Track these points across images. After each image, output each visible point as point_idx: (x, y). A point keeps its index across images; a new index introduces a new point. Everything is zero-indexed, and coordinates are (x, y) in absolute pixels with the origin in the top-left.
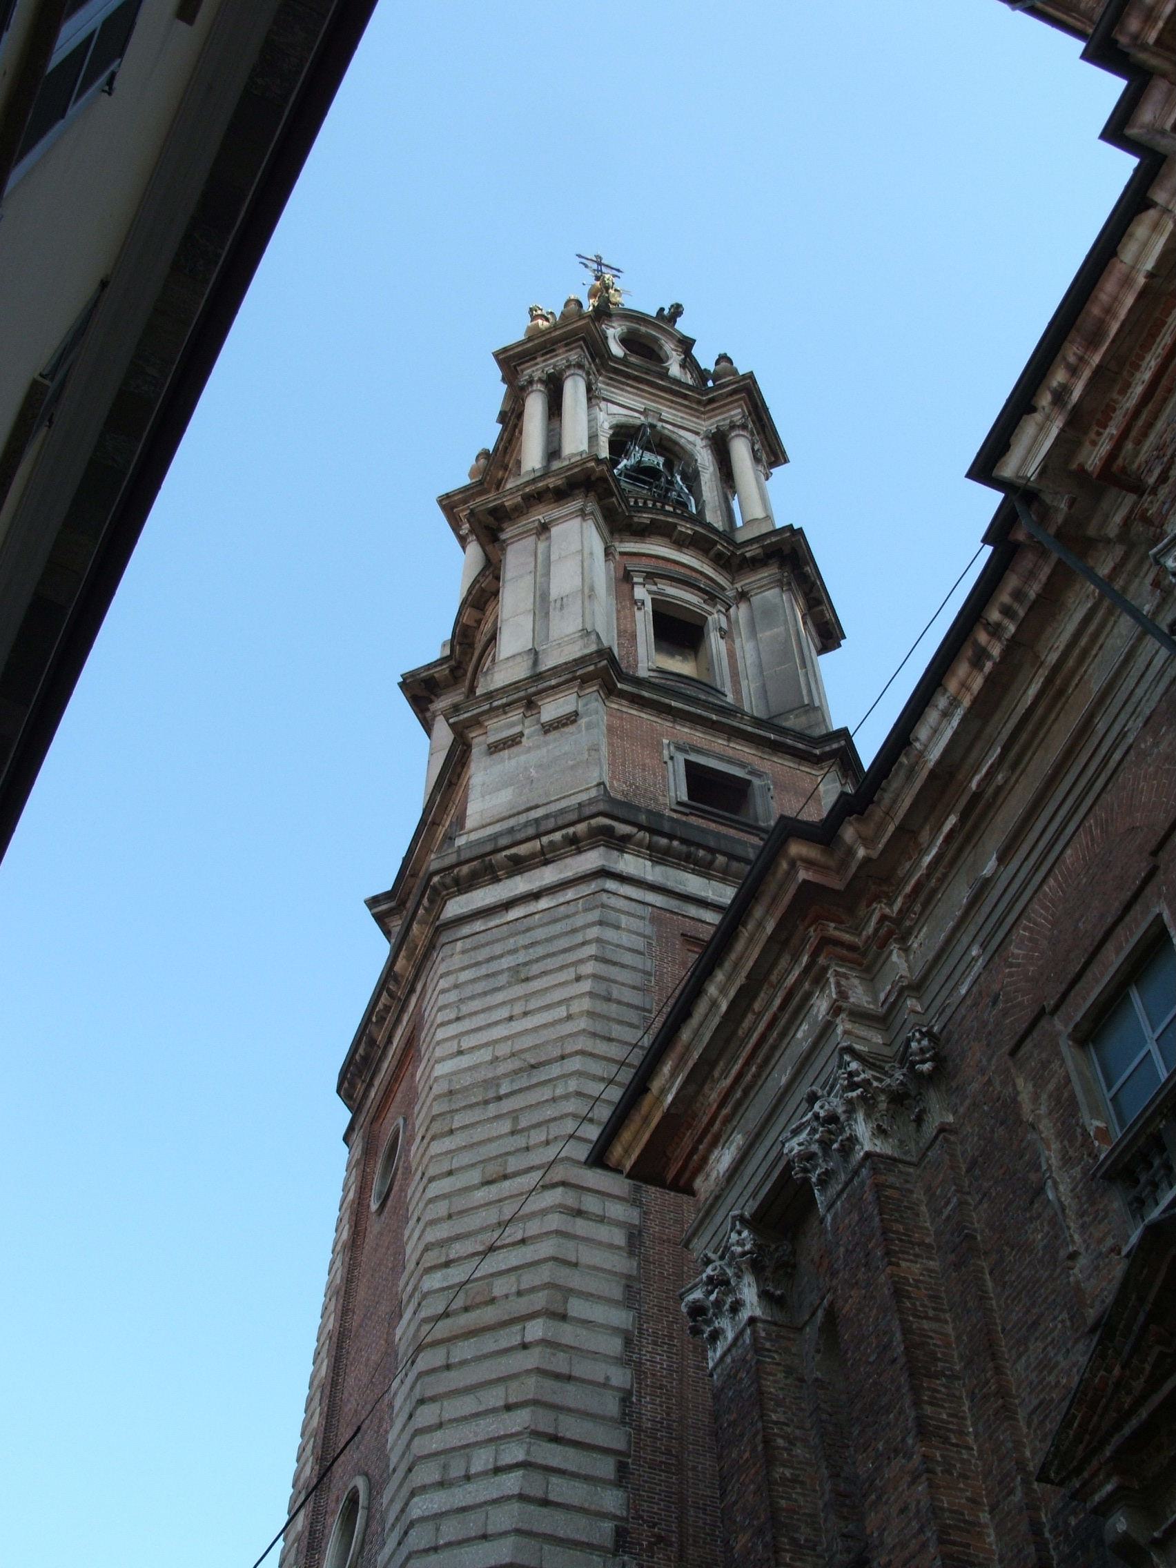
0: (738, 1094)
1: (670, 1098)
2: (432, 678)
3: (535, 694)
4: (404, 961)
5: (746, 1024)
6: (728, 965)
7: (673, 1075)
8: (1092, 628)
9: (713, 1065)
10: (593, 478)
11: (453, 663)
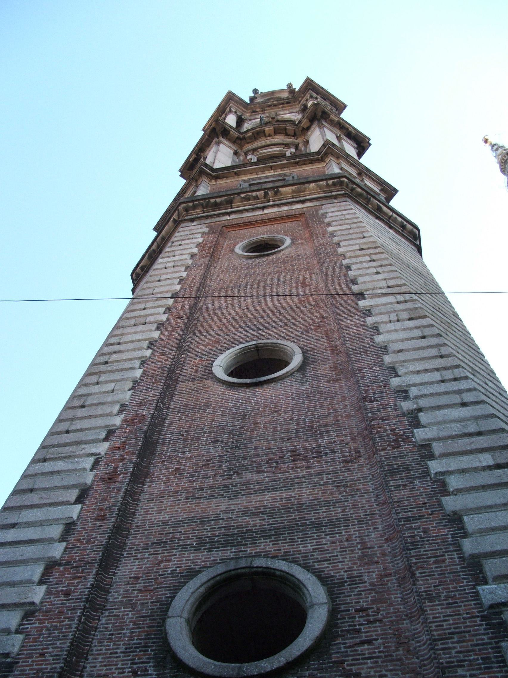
2: (229, 132)
3: (365, 173)
4: (291, 191)
10: (362, 144)
11: (241, 136)
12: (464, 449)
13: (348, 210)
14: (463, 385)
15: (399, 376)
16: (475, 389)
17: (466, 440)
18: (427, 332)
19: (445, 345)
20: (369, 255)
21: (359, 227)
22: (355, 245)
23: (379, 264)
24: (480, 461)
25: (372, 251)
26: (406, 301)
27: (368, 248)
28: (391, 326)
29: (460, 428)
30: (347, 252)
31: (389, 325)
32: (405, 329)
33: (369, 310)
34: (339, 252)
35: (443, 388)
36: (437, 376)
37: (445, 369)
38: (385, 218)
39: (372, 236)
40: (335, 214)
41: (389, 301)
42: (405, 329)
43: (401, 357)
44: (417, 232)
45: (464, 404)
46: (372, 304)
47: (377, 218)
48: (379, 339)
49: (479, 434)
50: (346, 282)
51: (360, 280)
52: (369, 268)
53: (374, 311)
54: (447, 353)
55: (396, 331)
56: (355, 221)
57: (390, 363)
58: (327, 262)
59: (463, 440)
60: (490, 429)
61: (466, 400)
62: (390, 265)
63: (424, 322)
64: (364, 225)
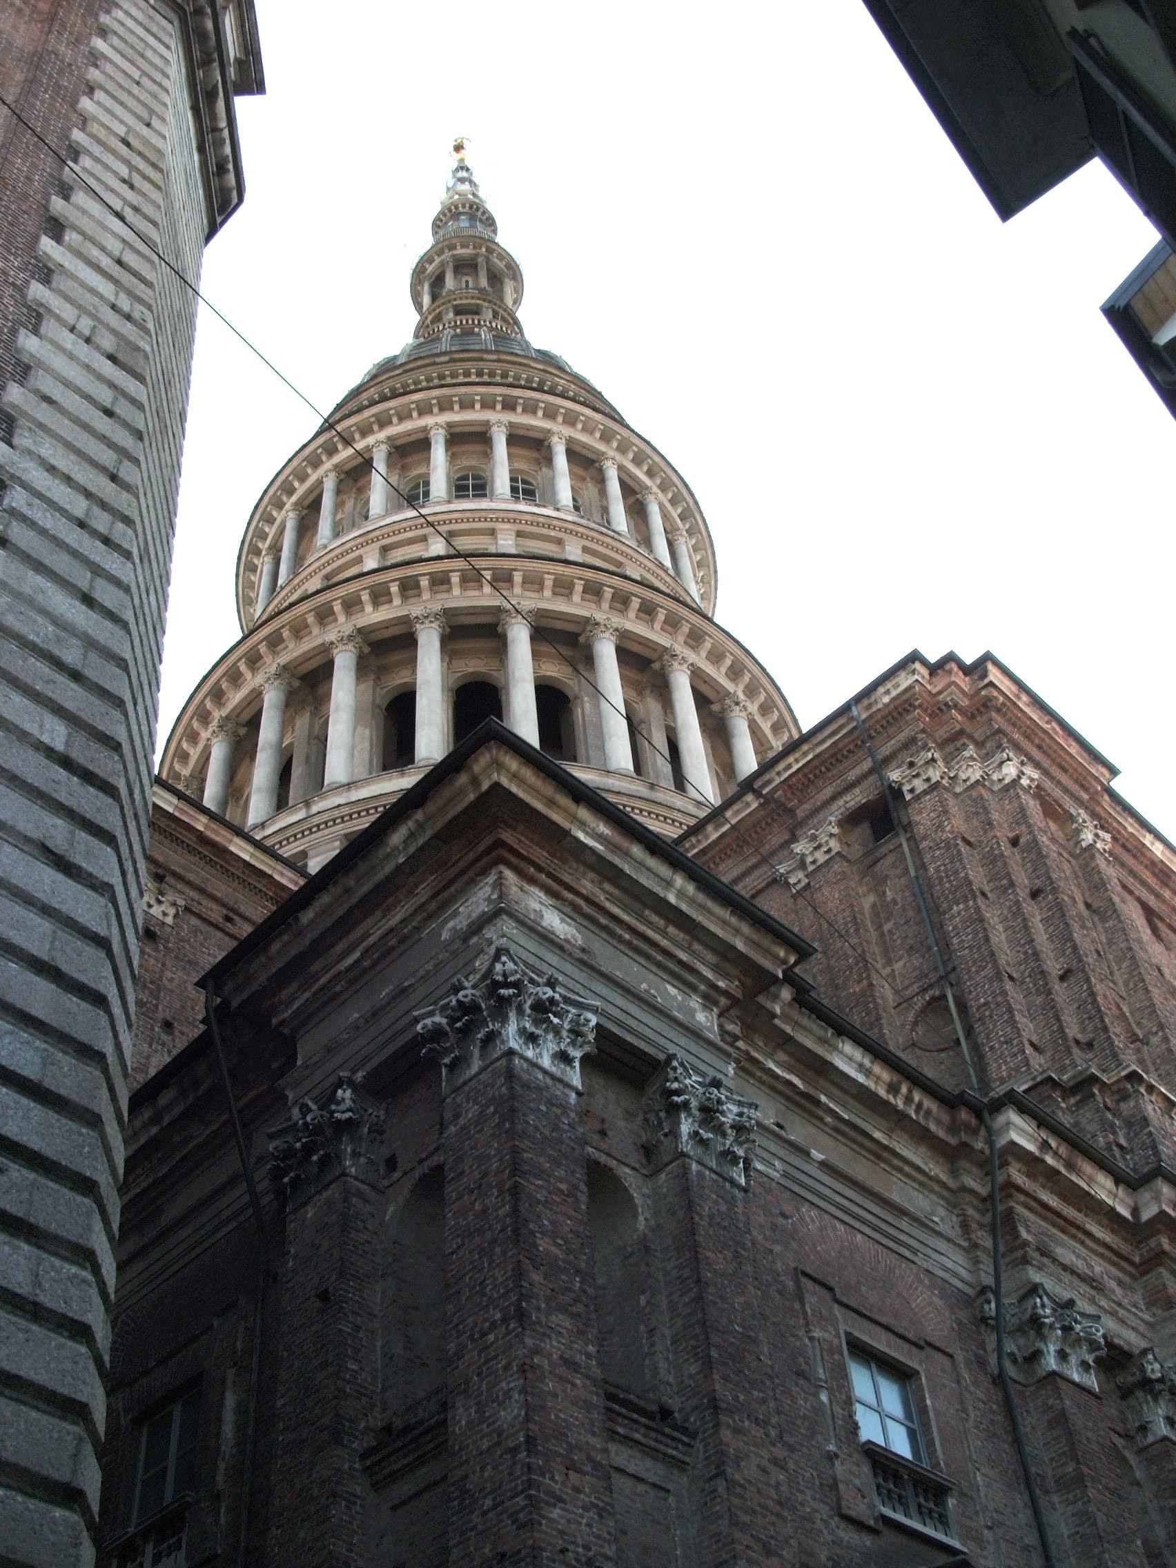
0: (603, 921)
1: (581, 836)
5: (655, 918)
6: (701, 897)
7: (599, 837)
8: (914, 1173)
9: (612, 881)
12: (29, 681)
13: (160, 41)
14: (112, 563)
15: (10, 445)
16: (127, 590)
17: (44, 669)
18: (122, 409)
19: (136, 462)
20: (133, 168)
21: (155, 96)
22: (122, 122)
23: (135, 203)
24: (41, 726)
25: (142, 165)
26: (128, 317)
27: (140, 154)
28: (68, 340)
29: (50, 636)
30: (95, 119)
31: (66, 333)
32: (88, 367)
33: (51, 271)
34: (80, 106)
35: (73, 536)
36: (79, 506)
37: (104, 505)
38: (206, 122)
39: (164, 138)
40: (130, 23)
41: (100, 290)
42: (88, 367)
43: (43, 413)
44: (235, 200)
45: (88, 600)
46: (66, 264)
47: (195, 109)
48: (29, 343)
49: (76, 676)
50: (51, 175)
51: (80, 197)
52: (112, 190)
53: (57, 280)
54: (128, 479)
55: (71, 356)
56: (158, 77)
57: (14, 406)
58: (43, 102)
59: (38, 664)
60: (101, 683)
61: (97, 595)
62: (155, 224)
63: (131, 386)
64: (167, 100)
